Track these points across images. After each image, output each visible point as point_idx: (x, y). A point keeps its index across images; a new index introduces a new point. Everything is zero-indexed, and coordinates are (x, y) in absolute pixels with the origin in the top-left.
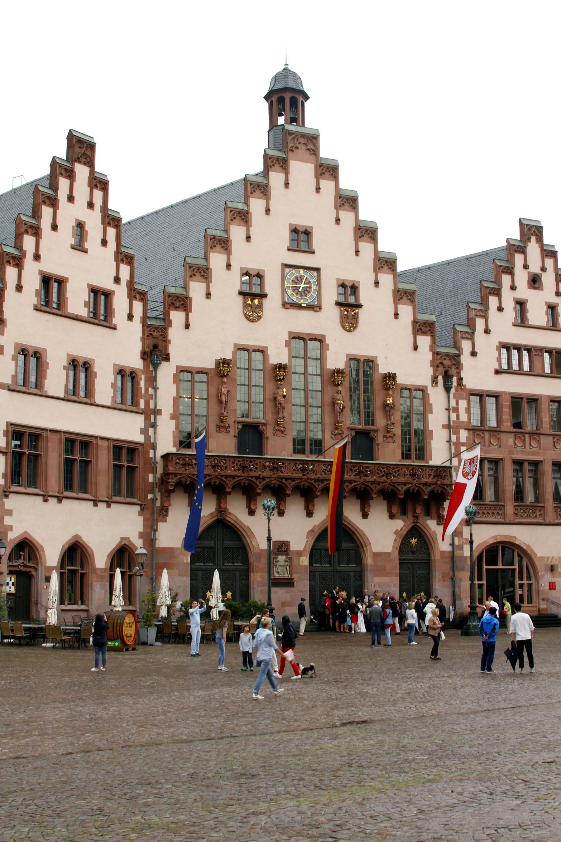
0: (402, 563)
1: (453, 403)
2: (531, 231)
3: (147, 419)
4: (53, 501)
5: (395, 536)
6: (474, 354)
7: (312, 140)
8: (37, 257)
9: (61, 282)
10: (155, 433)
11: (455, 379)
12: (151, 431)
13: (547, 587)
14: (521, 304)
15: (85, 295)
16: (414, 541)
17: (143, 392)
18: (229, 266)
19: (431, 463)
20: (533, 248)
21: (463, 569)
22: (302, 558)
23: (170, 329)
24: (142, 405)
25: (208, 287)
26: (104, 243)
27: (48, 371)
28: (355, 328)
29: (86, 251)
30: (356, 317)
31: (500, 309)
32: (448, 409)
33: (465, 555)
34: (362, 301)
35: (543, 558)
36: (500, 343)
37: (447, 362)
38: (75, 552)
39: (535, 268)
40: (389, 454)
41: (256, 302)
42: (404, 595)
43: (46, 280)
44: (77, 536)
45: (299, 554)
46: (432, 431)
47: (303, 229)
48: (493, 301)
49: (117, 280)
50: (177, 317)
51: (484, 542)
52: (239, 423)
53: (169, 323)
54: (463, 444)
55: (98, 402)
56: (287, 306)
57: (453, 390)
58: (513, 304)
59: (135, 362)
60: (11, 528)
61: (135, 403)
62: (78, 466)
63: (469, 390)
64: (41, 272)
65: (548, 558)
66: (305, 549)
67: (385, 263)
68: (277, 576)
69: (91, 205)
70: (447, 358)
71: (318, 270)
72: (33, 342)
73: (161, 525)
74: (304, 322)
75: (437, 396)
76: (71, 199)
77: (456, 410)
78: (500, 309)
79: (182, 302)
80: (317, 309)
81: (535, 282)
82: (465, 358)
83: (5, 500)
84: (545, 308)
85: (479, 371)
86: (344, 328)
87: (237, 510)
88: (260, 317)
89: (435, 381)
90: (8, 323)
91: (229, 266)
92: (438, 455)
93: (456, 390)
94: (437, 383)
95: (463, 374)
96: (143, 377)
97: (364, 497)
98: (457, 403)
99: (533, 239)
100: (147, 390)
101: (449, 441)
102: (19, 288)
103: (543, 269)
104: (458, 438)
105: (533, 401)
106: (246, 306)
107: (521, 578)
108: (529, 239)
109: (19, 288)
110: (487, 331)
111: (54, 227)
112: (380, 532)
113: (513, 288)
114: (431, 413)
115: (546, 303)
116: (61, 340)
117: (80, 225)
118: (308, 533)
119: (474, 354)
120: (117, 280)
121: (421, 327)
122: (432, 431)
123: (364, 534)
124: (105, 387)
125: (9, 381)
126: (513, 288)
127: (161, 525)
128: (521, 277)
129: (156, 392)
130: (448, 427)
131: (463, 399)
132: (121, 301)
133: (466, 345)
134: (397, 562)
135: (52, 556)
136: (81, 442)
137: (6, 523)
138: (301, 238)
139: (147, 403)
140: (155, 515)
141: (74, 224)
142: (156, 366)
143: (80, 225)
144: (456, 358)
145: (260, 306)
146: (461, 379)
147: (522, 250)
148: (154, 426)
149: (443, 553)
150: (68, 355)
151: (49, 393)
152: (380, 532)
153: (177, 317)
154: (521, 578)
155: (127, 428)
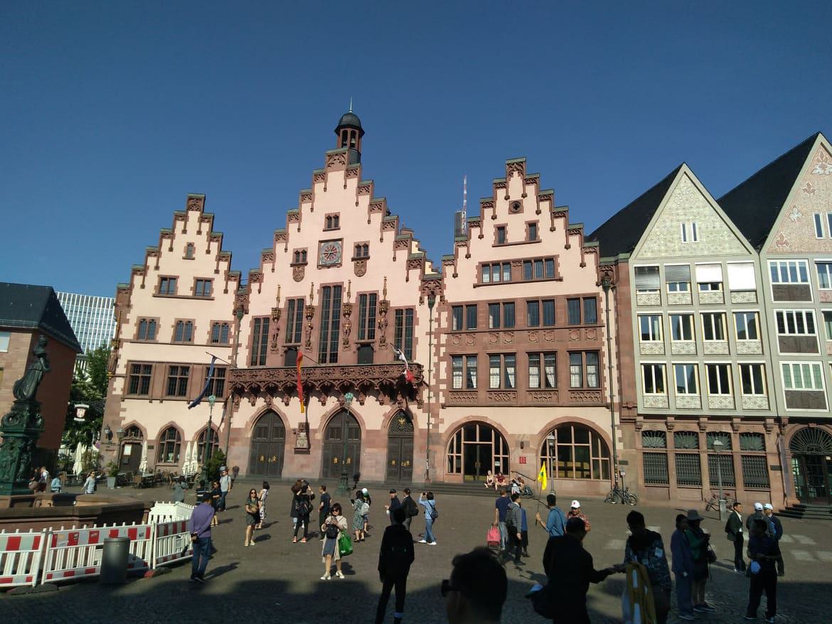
0: (391, 437)
1: (435, 315)
4: (156, 403)
5: (384, 418)
6: (455, 276)
8: (157, 268)
9: (174, 279)
10: (236, 358)
11: (438, 298)
13: (517, 461)
14: (501, 229)
15: (192, 284)
17: (233, 334)
18: (286, 250)
19: (415, 362)
20: (516, 182)
21: (438, 443)
22: (317, 435)
23: (250, 295)
24: (231, 341)
25: (273, 266)
26: (208, 252)
27: (160, 330)
28: (364, 273)
29: (194, 259)
30: (365, 266)
31: (481, 237)
32: (431, 321)
33: (440, 432)
34: (371, 253)
35: (513, 435)
36: (480, 263)
37: (432, 285)
40: (383, 356)
41: (301, 269)
42: (394, 462)
44: (173, 422)
45: (315, 431)
46: (417, 338)
47: (334, 215)
48: (475, 232)
49: (217, 271)
50: (255, 286)
51: (458, 422)
52: (284, 347)
53: (250, 291)
54: (443, 346)
55: (195, 343)
56: (320, 267)
57: (436, 305)
58: (493, 230)
59: (229, 317)
60: (124, 418)
62: (178, 382)
63: (450, 303)
64: (159, 276)
65: (520, 435)
66: (319, 429)
68: (299, 446)
69: (199, 232)
70: (432, 283)
71: (341, 240)
72: (149, 313)
73: (235, 413)
76: (184, 231)
77: (438, 320)
80: (338, 265)
81: (516, 207)
82: (448, 280)
83: (122, 403)
84: (525, 226)
86: (356, 275)
87: (277, 402)
88: (303, 277)
90: (134, 307)
91: (286, 250)
93: (439, 305)
94: (423, 302)
95: (446, 293)
96: (233, 325)
97: (365, 390)
98: (440, 315)
99: (516, 173)
100: (235, 333)
101: (430, 345)
102: (143, 286)
103: (524, 196)
104: (439, 341)
105: (510, 303)
106: (294, 272)
107: (497, 452)
108: (511, 174)
109: (143, 286)
110: (468, 256)
111: (171, 249)
112: (373, 414)
113: (494, 218)
114: (418, 325)
115: (526, 222)
116: (168, 313)
117: (190, 245)
118: (322, 417)
119: (455, 276)
120: (217, 271)
121: (414, 262)
122: (417, 338)
123: (361, 417)
124: (202, 333)
125: (131, 337)
126: (494, 218)
127: (235, 413)
129: (238, 333)
130: (430, 333)
131: (444, 311)
132: (219, 283)
133: (449, 270)
134: (385, 438)
135: (152, 433)
136: (182, 367)
137: (121, 416)
138: (332, 221)
139: (234, 341)
141: (186, 245)
142: (240, 318)
143: (190, 245)
144: (440, 282)
145: (303, 271)
146: (442, 297)
147: (504, 185)
149: (421, 430)
150: (194, 320)
151: (160, 342)
152: (373, 414)
153: (255, 286)
154: (497, 452)
155: (223, 356)
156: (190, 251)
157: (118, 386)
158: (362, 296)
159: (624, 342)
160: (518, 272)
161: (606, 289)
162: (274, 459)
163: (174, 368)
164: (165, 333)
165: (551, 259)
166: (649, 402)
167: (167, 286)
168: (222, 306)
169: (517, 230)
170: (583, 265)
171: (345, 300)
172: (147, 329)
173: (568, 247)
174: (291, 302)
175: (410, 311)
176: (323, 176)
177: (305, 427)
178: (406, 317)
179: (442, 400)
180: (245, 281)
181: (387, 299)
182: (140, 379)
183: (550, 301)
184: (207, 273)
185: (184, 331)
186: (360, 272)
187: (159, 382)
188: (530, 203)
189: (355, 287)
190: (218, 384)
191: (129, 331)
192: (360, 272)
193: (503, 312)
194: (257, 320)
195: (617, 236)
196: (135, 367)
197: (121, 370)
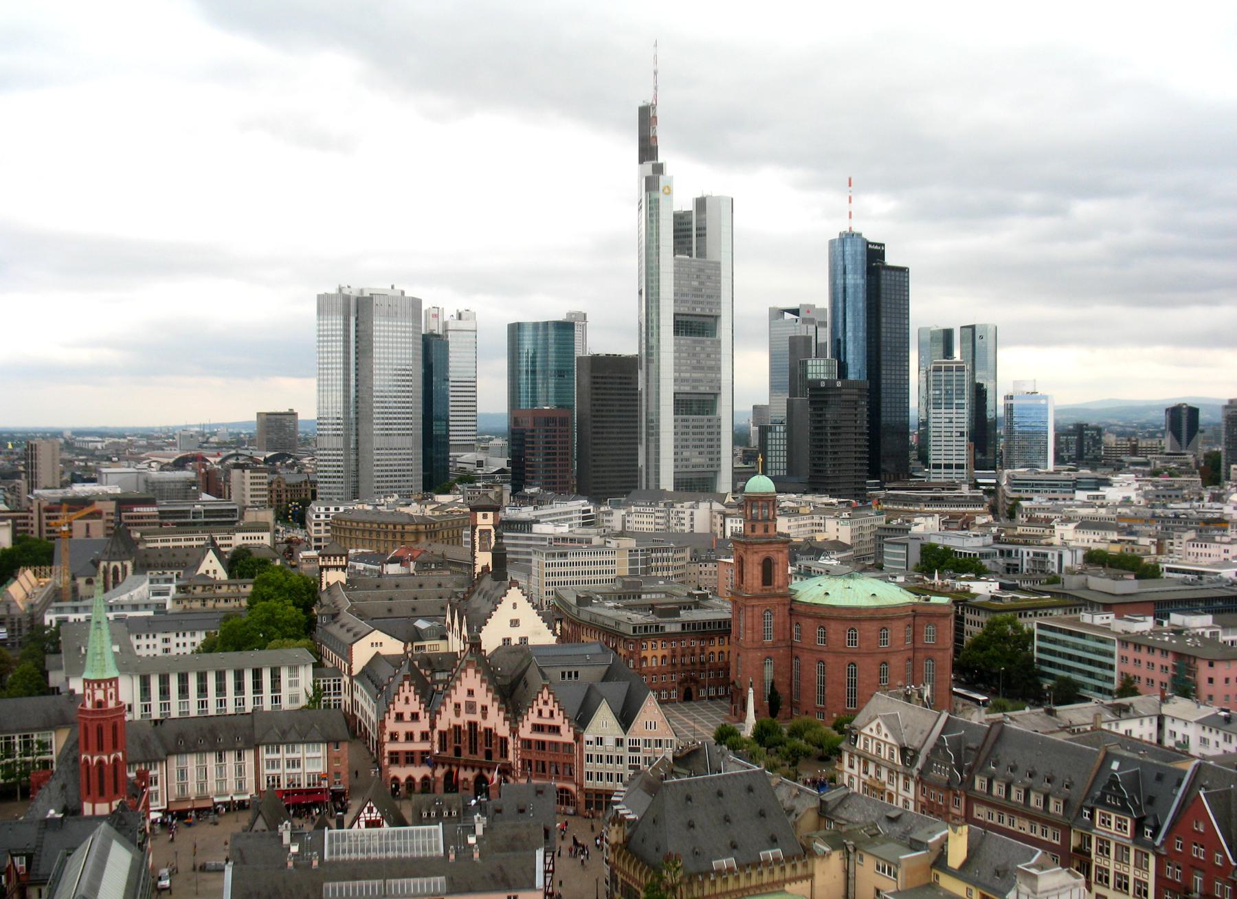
14: (540, 712)
20: (545, 692)
38: (410, 779)
39: (546, 697)
43: (397, 715)
62: (410, 758)
74: (472, 718)
75: (510, 740)
79: (440, 713)
85: (525, 732)
92: (511, 758)
105: (543, 742)
116: (402, 729)
128: (541, 701)
135: (403, 780)
138: (471, 693)
140: (434, 768)
155: (426, 746)
156: (407, 700)
157: (386, 761)
158: (486, 729)
159: (581, 763)
160: (546, 729)
163: (407, 753)
164: (402, 738)
166: (589, 784)
167: (400, 717)
168: (424, 725)
169: (546, 713)
172: (394, 737)
174: (455, 726)
175: (506, 739)
176: (465, 671)
177: (466, 780)
178: (504, 741)
180: (434, 714)
182: (395, 758)
183: (556, 743)
184: (416, 709)
185: (409, 737)
186: (484, 716)
187: (402, 758)
188: (551, 702)
189: (483, 725)
190: (424, 758)
191: (387, 738)
192: (484, 716)
193: (542, 745)
194: (440, 732)
195: (582, 719)
196: (391, 753)
197: (386, 754)
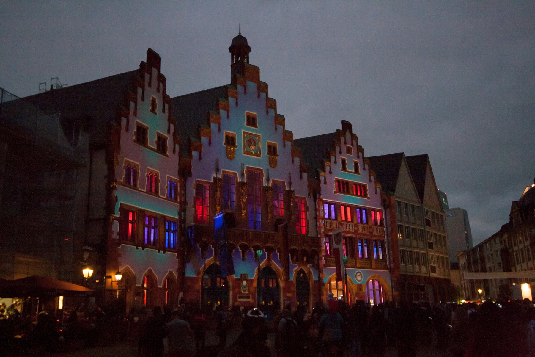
2: (346, 126)
3: (181, 207)
7: (256, 70)
8: (135, 114)
12: (183, 213)
14: (344, 162)
16: (302, 275)
31: (335, 162)
38: (150, 278)
57: (317, 200)
61: (176, 198)
67: (288, 135)
78: (335, 162)
86: (271, 166)
89: (309, 194)
99: (348, 131)
148: (185, 211)
161: (385, 208)
162: (219, 303)
165: (364, 186)
170: (376, 193)
171: (265, 184)
173: (370, 181)
179: (324, 262)
181: (292, 189)
186: (273, 163)
188: (354, 150)
